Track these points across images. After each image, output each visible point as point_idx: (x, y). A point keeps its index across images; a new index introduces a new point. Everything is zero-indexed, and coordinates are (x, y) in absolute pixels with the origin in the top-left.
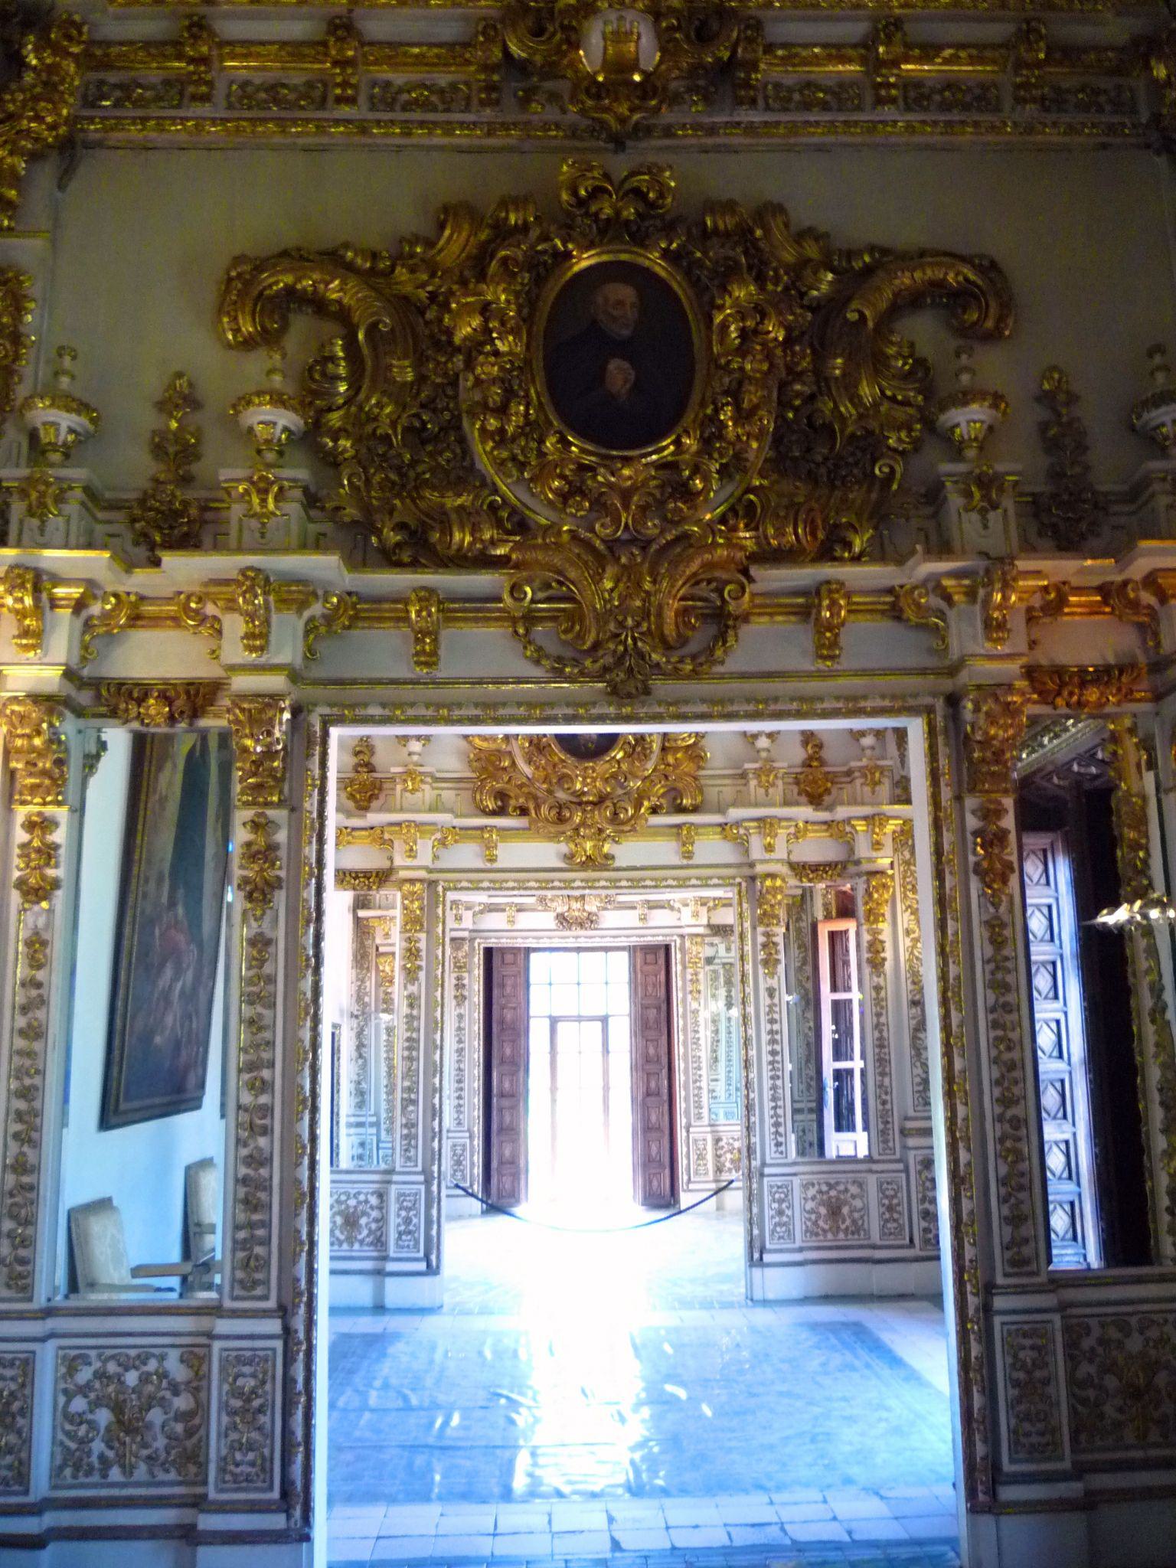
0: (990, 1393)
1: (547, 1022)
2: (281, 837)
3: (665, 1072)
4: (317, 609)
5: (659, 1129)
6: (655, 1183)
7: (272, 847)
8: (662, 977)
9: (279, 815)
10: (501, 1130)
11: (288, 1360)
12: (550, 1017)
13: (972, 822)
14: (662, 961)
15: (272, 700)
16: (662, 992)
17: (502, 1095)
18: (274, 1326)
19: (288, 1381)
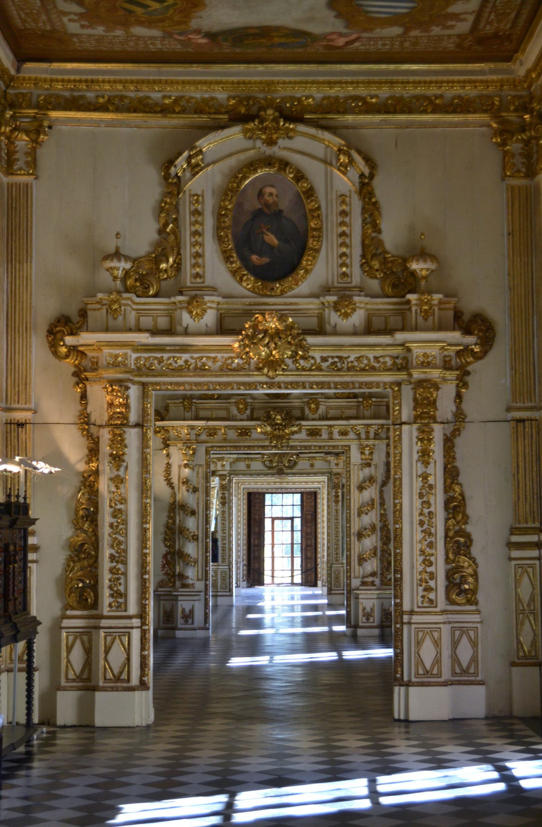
0: (331, 577)
1: (270, 519)
2: (226, 495)
3: (313, 539)
4: (232, 460)
5: (311, 558)
6: (309, 578)
7: (225, 497)
8: (313, 504)
9: (226, 492)
10: (254, 558)
11: (230, 572)
12: (271, 517)
13: (334, 494)
14: (313, 498)
15: (224, 475)
16: (313, 509)
17: (255, 546)
18: (227, 567)
19: (230, 575)
